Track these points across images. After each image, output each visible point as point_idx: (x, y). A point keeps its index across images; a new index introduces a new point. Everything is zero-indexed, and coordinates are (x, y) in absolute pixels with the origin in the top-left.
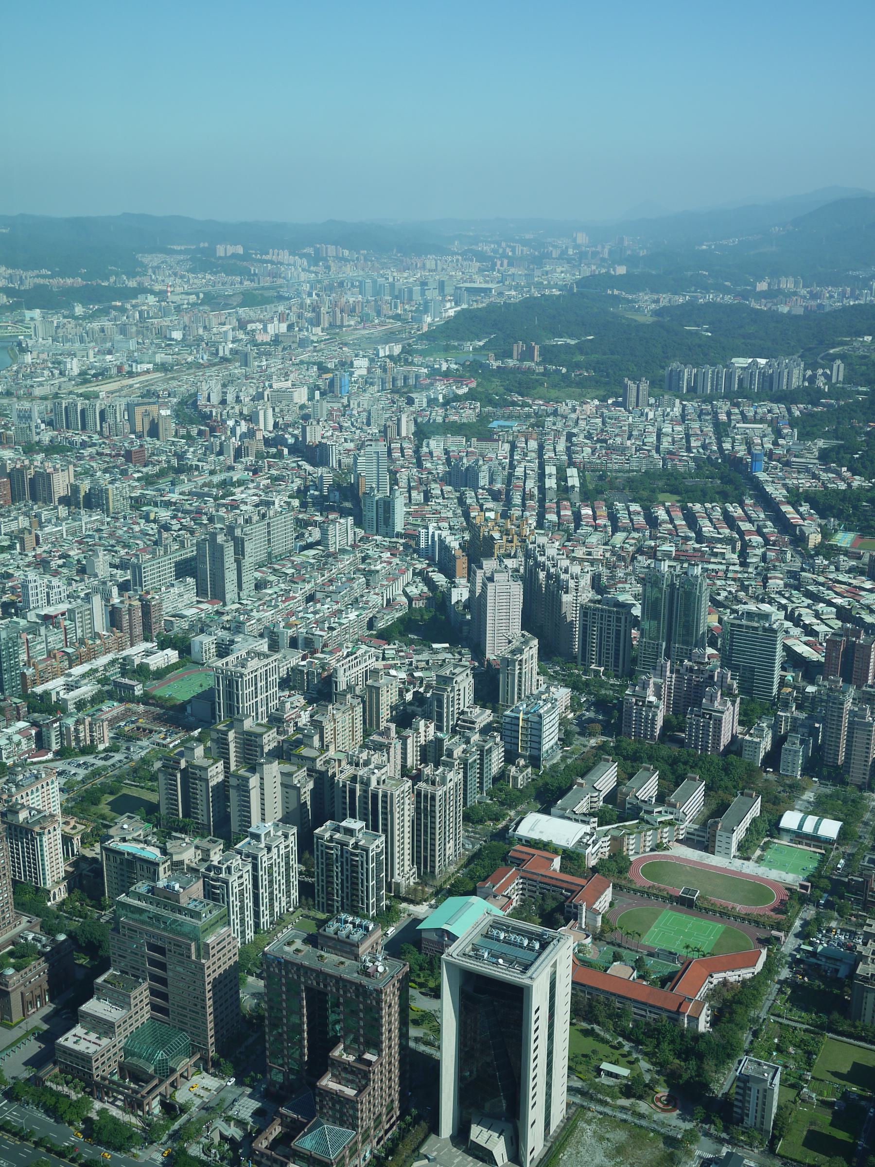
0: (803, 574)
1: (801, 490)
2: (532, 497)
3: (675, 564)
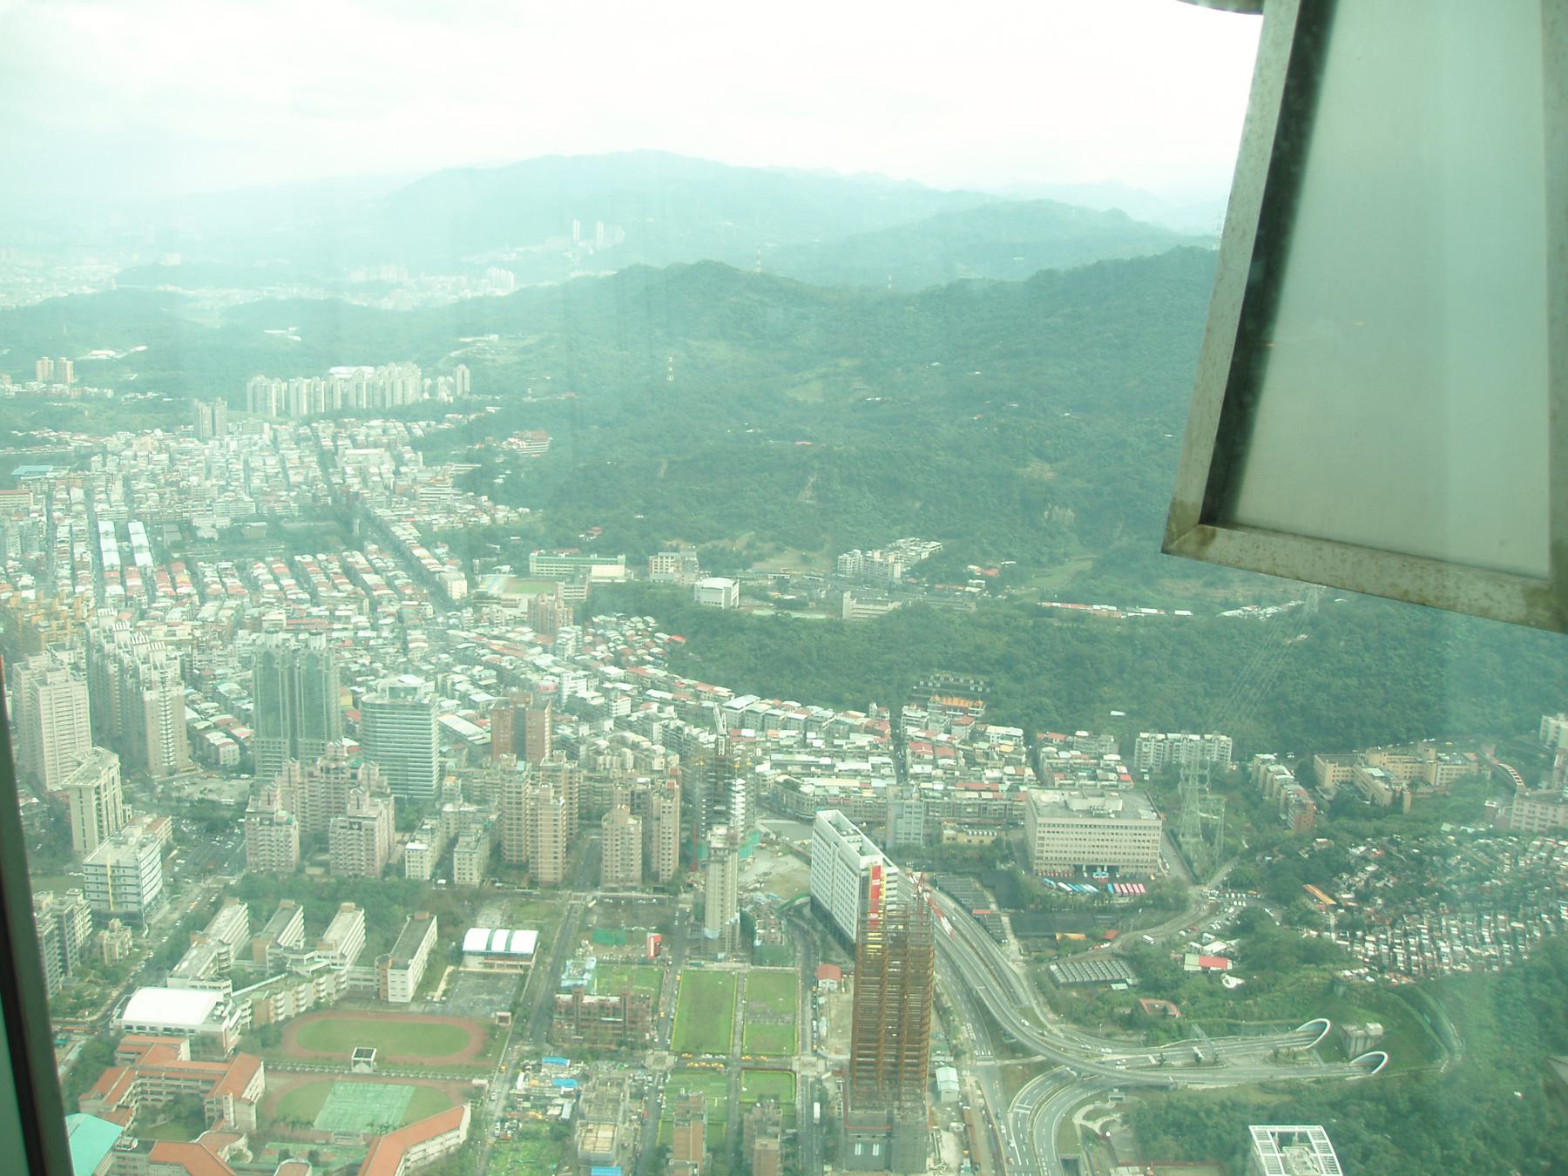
0: (451, 632)
1: (435, 529)
2: (85, 566)
3: (288, 636)
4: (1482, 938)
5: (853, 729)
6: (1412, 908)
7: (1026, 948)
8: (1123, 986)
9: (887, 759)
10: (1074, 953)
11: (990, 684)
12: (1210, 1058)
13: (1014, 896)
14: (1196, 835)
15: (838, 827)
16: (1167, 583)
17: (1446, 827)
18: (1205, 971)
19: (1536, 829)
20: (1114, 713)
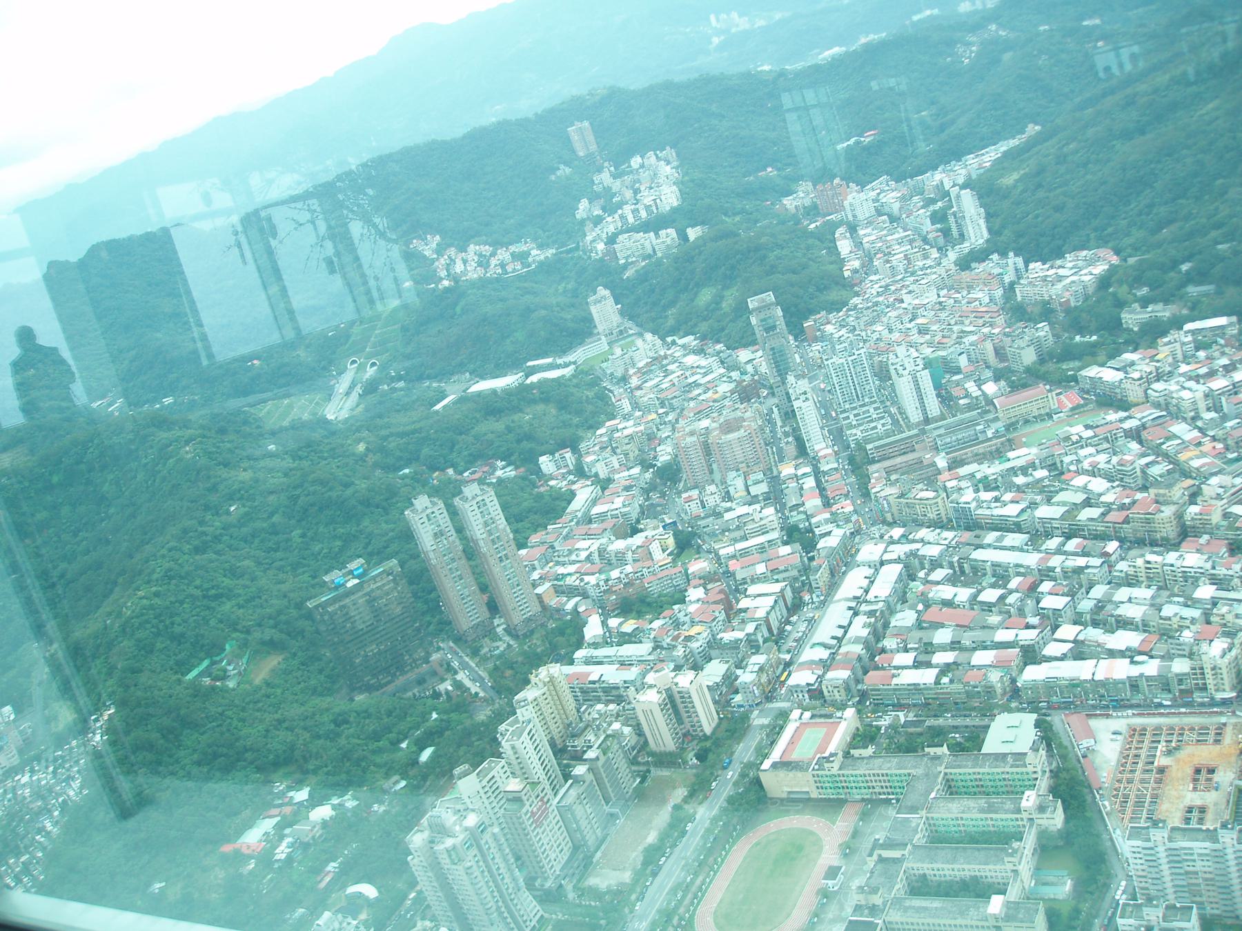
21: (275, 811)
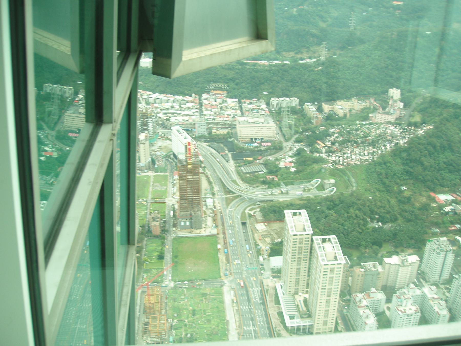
4: (364, 153)
5: (188, 102)
6: (346, 146)
7: (236, 164)
8: (262, 173)
9: (197, 110)
10: (249, 163)
11: (228, 86)
12: (286, 192)
13: (232, 148)
14: (286, 128)
15: (179, 131)
16: (284, 53)
17: (358, 122)
18: (286, 167)
19: (383, 122)
20: (264, 93)
21: (455, 195)
